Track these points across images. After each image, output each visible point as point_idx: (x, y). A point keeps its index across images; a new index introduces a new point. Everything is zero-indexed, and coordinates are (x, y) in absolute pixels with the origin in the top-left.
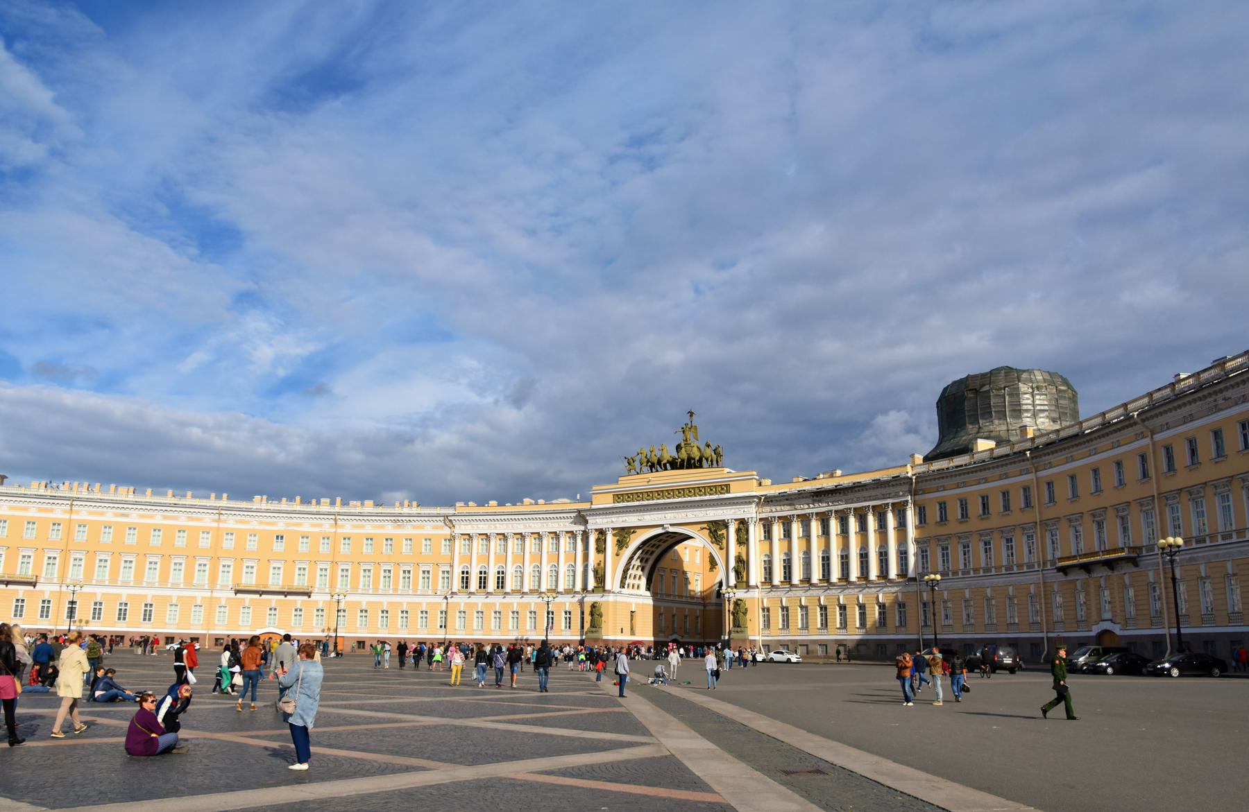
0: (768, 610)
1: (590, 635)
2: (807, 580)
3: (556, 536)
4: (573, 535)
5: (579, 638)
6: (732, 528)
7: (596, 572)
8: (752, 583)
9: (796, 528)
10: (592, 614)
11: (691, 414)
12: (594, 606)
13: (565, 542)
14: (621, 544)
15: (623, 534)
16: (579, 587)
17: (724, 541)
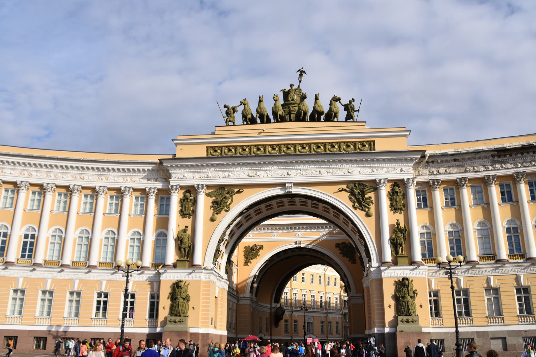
0: (436, 294)
1: (170, 327)
2: (490, 255)
3: (119, 193)
4: (144, 193)
5: (146, 331)
6: (384, 191)
7: (179, 241)
8: (418, 257)
9: (467, 195)
10: (173, 297)
11: (301, 73)
12: (177, 286)
13: (129, 202)
14: (219, 206)
15: (222, 196)
16: (148, 261)
17: (372, 207)
